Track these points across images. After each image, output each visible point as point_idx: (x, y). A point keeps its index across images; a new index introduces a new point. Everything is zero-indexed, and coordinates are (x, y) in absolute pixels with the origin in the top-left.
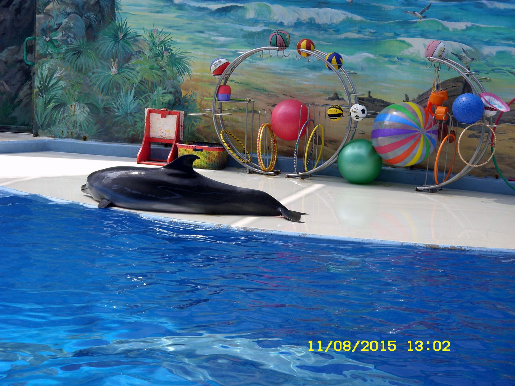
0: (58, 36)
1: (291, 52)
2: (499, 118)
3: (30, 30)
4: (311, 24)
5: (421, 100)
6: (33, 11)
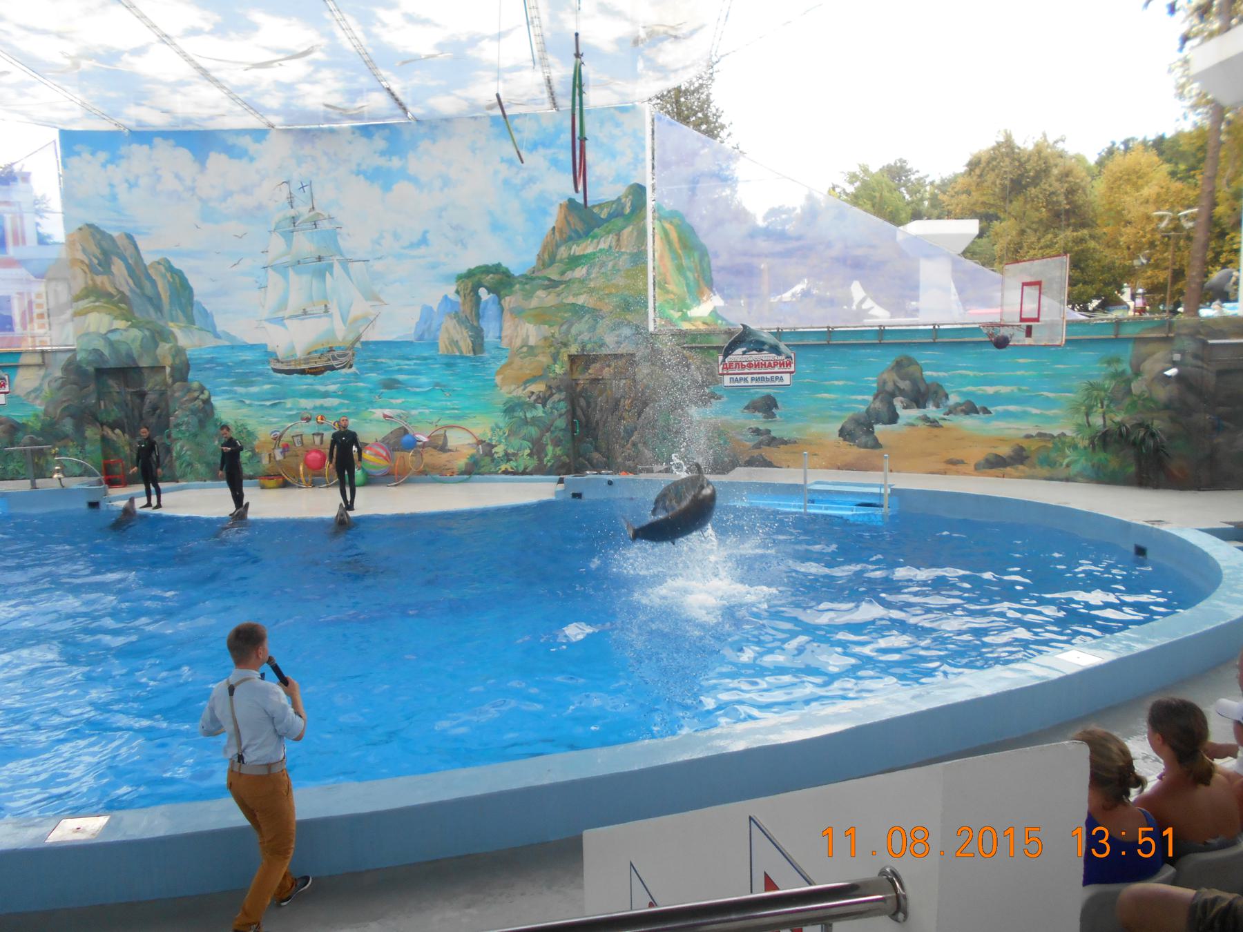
0: (183, 428)
1: (313, 422)
2: (424, 445)
3: (167, 426)
4: (322, 407)
5: (384, 440)
6: (168, 416)
